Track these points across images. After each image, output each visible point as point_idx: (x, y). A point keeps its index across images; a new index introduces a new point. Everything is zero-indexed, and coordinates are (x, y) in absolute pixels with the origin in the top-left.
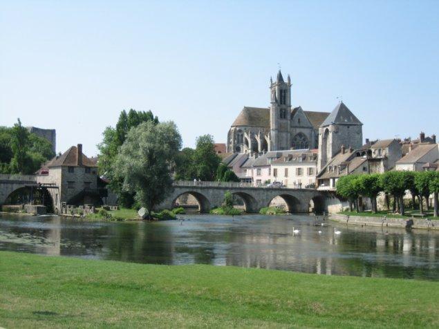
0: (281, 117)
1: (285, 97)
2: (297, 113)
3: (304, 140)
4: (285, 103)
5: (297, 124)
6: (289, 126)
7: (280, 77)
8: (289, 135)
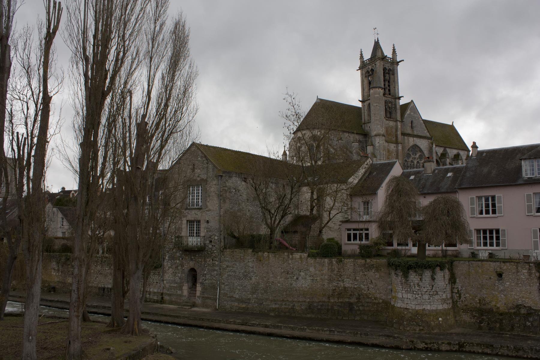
1: (389, 82)
2: (408, 112)
5: (409, 131)
6: (399, 133)
8: (400, 148)
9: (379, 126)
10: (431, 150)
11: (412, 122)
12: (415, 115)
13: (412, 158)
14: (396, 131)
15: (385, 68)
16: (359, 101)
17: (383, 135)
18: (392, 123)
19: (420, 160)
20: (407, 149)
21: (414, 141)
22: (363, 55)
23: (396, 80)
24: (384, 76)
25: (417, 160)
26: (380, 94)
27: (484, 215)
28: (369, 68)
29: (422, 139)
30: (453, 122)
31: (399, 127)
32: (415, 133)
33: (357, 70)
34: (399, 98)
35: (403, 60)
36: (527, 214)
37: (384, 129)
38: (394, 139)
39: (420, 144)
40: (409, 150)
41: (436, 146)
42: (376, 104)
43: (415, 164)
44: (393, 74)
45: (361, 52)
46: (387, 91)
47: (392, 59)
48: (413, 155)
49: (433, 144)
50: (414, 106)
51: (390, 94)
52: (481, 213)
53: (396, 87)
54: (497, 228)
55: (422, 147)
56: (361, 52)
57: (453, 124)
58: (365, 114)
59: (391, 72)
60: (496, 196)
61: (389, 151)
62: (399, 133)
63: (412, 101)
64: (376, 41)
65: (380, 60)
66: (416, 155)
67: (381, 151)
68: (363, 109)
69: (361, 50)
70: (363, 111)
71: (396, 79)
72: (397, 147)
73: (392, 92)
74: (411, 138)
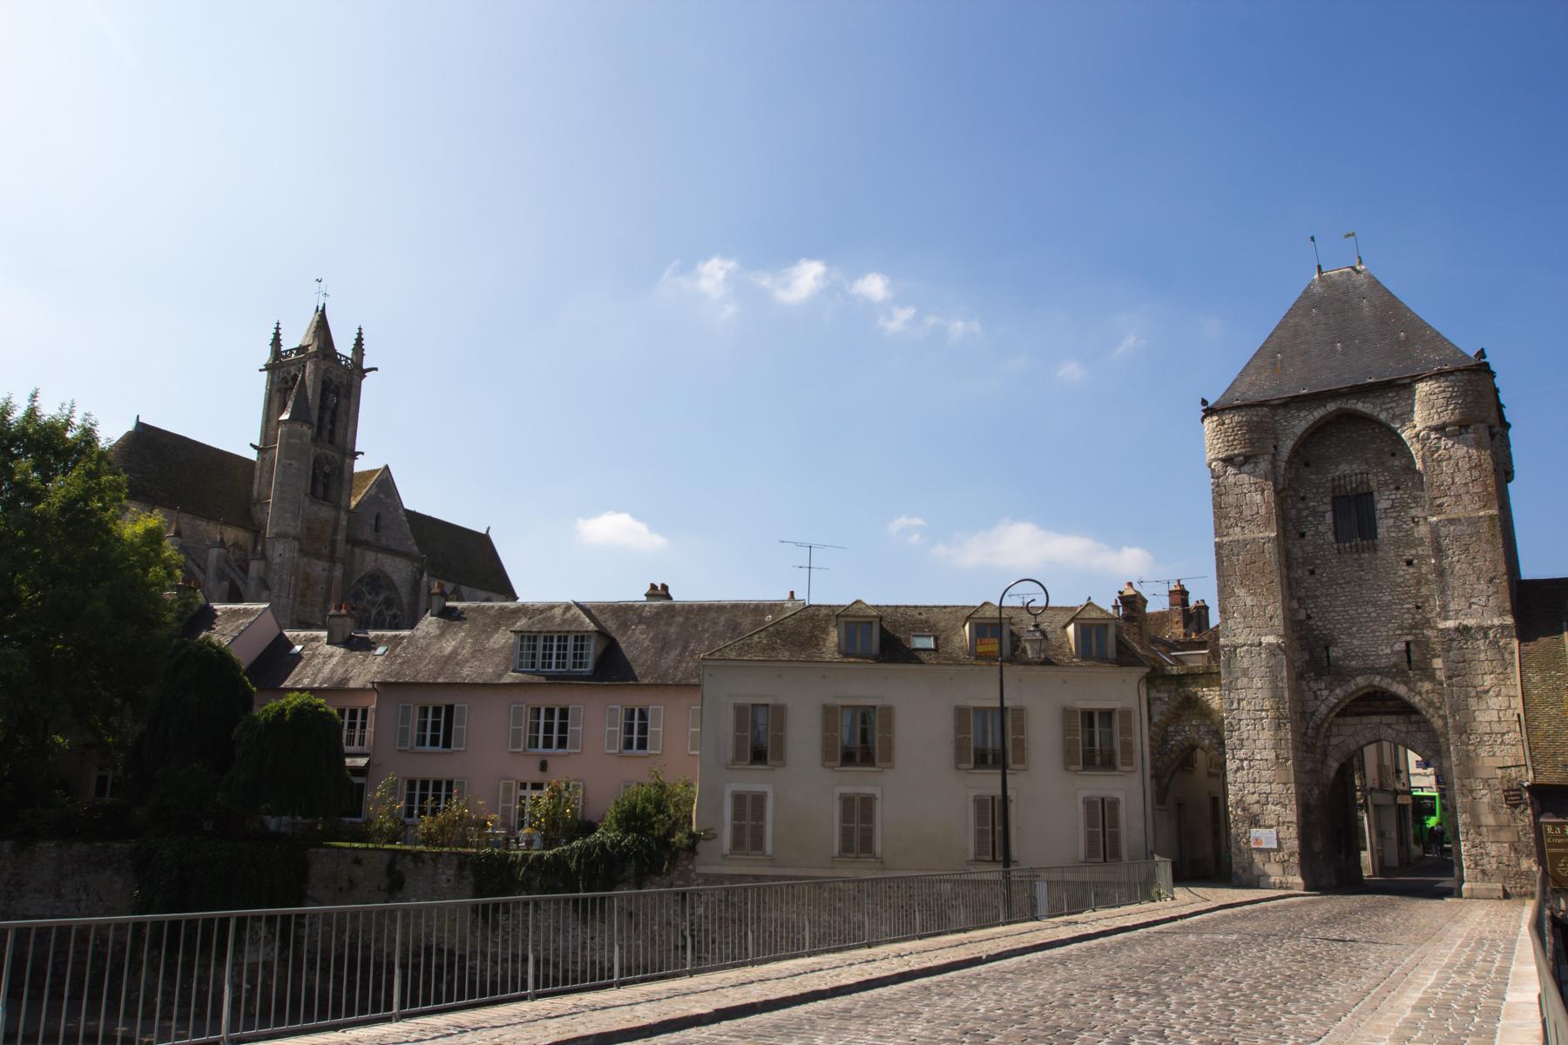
0: (313, 493)
1: (334, 413)
3: (388, 603)
4: (331, 442)
5: (367, 533)
6: (340, 537)
7: (322, 327)
8: (338, 572)
9: (288, 515)
10: (416, 584)
11: (378, 518)
12: (389, 500)
13: (368, 601)
14: (335, 531)
15: (330, 380)
16: (252, 445)
17: (295, 538)
18: (325, 512)
19: (387, 609)
20: (358, 577)
21: (377, 560)
22: (281, 337)
23: (351, 413)
24: (323, 398)
25: (379, 608)
26: (304, 439)
27: (428, 747)
28: (289, 373)
29: (397, 559)
30: (489, 529)
31: (344, 523)
32: (383, 542)
33: (261, 370)
34: (354, 455)
35: (376, 369)
36: (510, 750)
37: (299, 523)
38: (326, 551)
39: (391, 569)
40: (360, 581)
41: (429, 575)
42: (288, 462)
43: (373, 617)
44: (348, 397)
45: (278, 329)
46: (326, 433)
47: (349, 361)
48: (370, 594)
49: (422, 575)
50: (390, 479)
51: (331, 442)
52: (422, 741)
53: (350, 429)
54: (448, 776)
55: (395, 577)
56: (278, 329)
57: (488, 531)
58: (263, 480)
59: (343, 391)
60: (456, 706)
61: (307, 577)
62: (340, 537)
63: (387, 468)
64: (320, 309)
65: (317, 357)
66: (377, 594)
67: (285, 576)
68: (258, 467)
69: (278, 324)
70: (257, 473)
71: (353, 408)
72: (331, 570)
73: (338, 437)
74: (372, 553)
